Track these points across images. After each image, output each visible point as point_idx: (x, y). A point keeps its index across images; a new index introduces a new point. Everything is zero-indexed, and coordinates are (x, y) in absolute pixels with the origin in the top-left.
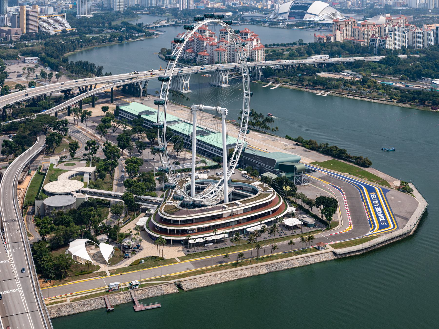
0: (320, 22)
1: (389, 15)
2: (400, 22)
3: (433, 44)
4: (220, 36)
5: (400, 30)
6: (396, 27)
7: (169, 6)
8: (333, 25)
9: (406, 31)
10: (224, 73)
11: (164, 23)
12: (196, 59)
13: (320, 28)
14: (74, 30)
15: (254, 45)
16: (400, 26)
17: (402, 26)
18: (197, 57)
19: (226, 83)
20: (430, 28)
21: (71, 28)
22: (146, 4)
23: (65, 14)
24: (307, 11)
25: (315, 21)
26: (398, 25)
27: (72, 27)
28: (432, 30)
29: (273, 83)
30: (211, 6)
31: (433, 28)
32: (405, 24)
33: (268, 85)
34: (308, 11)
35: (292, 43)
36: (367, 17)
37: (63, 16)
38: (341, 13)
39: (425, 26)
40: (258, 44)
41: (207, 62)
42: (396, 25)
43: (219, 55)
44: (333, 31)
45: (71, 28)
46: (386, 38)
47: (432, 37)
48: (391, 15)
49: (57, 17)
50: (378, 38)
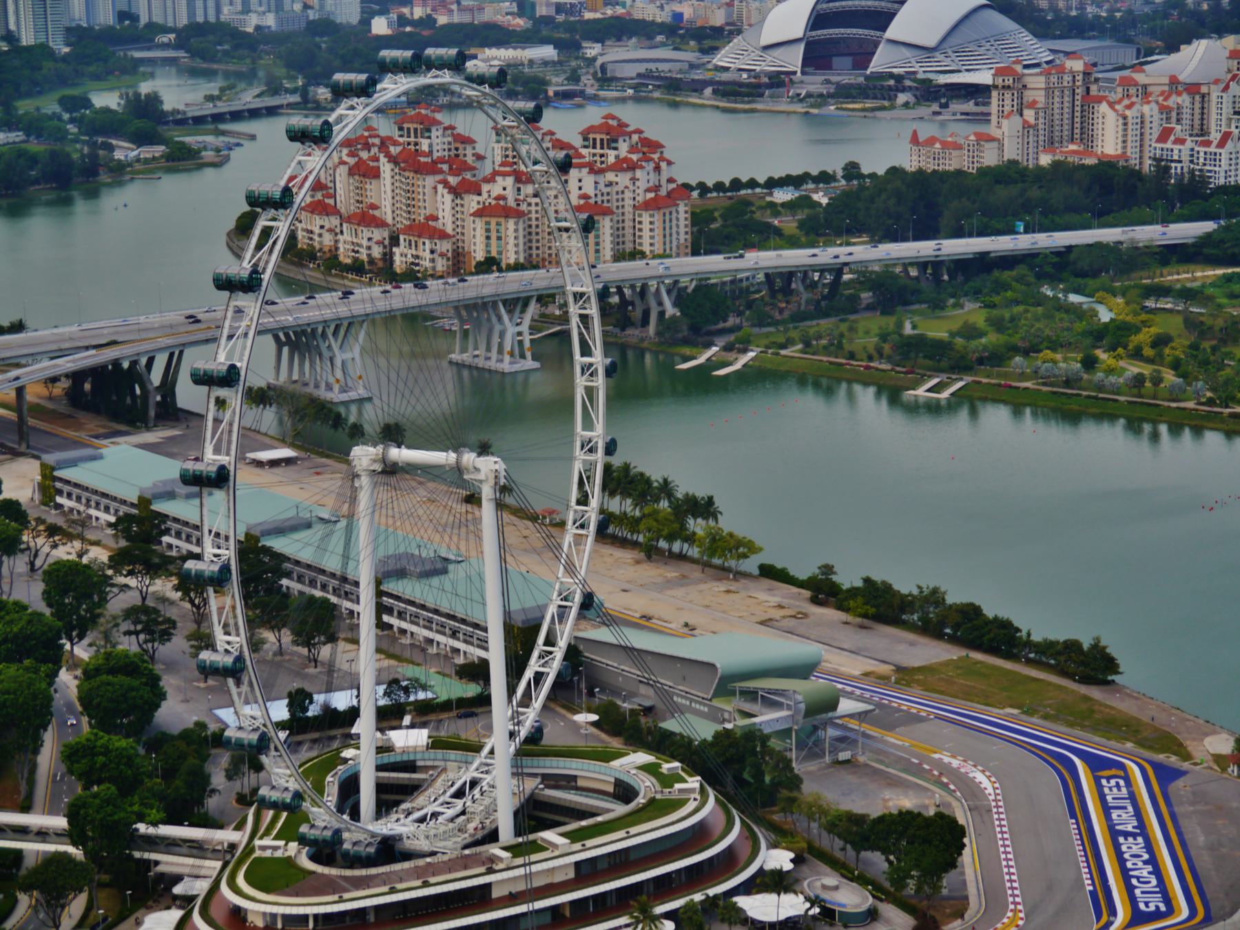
0: (943, 79)
4: (498, 152)
7: (270, 21)
8: (994, 94)
10: (510, 312)
11: (248, 98)
12: (392, 254)
13: (945, 106)
15: (642, 184)
18: (398, 245)
19: (523, 356)
22: (170, 11)
24: (884, 28)
25: (921, 76)
29: (728, 348)
30: (466, 18)
33: (701, 360)
34: (893, 32)
35: (815, 172)
36: (1150, 52)
38: (1035, 35)
40: (664, 182)
41: (441, 265)
43: (494, 235)
44: (994, 118)
46: (1221, 144)
50: (1189, 144)
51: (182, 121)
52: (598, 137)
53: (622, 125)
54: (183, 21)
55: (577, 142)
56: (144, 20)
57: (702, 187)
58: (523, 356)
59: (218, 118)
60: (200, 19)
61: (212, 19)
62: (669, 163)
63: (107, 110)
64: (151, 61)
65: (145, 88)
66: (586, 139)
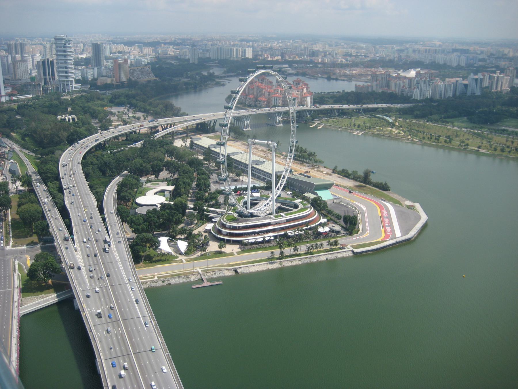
1: (419, 69)
2: (426, 76)
3: (451, 95)
4: (277, 84)
5: (426, 82)
6: (423, 80)
9: (431, 84)
10: (278, 116)
12: (256, 103)
14: (157, 79)
16: (426, 79)
17: (428, 79)
20: (451, 81)
21: (155, 78)
23: (150, 66)
26: (425, 78)
27: (156, 77)
28: (453, 83)
30: (271, 59)
31: (453, 82)
32: (431, 78)
33: (314, 126)
37: (149, 68)
39: (447, 80)
42: (424, 78)
45: (155, 78)
46: (414, 89)
47: (452, 89)
48: (421, 69)
49: (143, 68)
50: (408, 89)
51: (218, 77)
52: (296, 82)
53: (300, 80)
54: (219, 59)
55: (292, 83)
56: (212, 58)
57: (315, 93)
58: (280, 123)
59: (225, 77)
60: (222, 58)
61: (224, 58)
62: (309, 88)
63: (204, 75)
64: (213, 66)
65: (211, 71)
66: (293, 83)
